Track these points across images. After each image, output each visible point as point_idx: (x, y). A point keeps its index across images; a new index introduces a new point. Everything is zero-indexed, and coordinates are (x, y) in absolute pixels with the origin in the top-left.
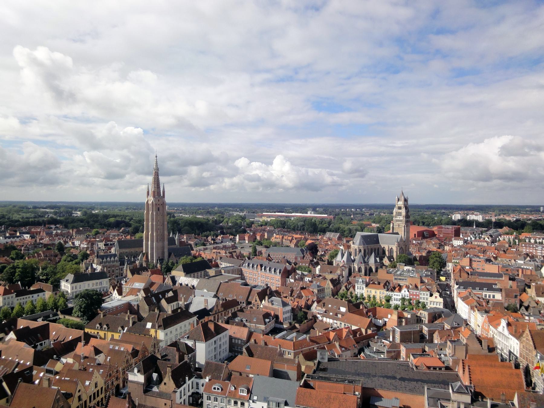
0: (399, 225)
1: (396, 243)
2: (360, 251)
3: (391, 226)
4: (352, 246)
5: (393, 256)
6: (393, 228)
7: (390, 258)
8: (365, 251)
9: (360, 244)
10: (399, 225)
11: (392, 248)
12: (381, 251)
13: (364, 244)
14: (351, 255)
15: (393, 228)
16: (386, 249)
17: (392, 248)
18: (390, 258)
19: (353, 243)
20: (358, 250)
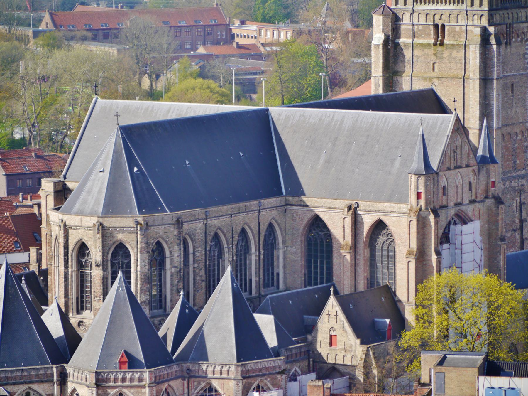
0: (439, 30)
1: (415, 184)
2: (117, 258)
3: (378, 38)
4: (52, 219)
5: (389, 292)
6: (392, 51)
7: (377, 319)
8: (157, 255)
9: (112, 206)
10: (439, 30)
11: (379, 226)
12: (290, 256)
13: (146, 203)
14: (42, 297)
15: (392, 51)
16: (339, 227)
17: (379, 226)
18: (377, 319)
19: (62, 193)
20: (96, 254)
